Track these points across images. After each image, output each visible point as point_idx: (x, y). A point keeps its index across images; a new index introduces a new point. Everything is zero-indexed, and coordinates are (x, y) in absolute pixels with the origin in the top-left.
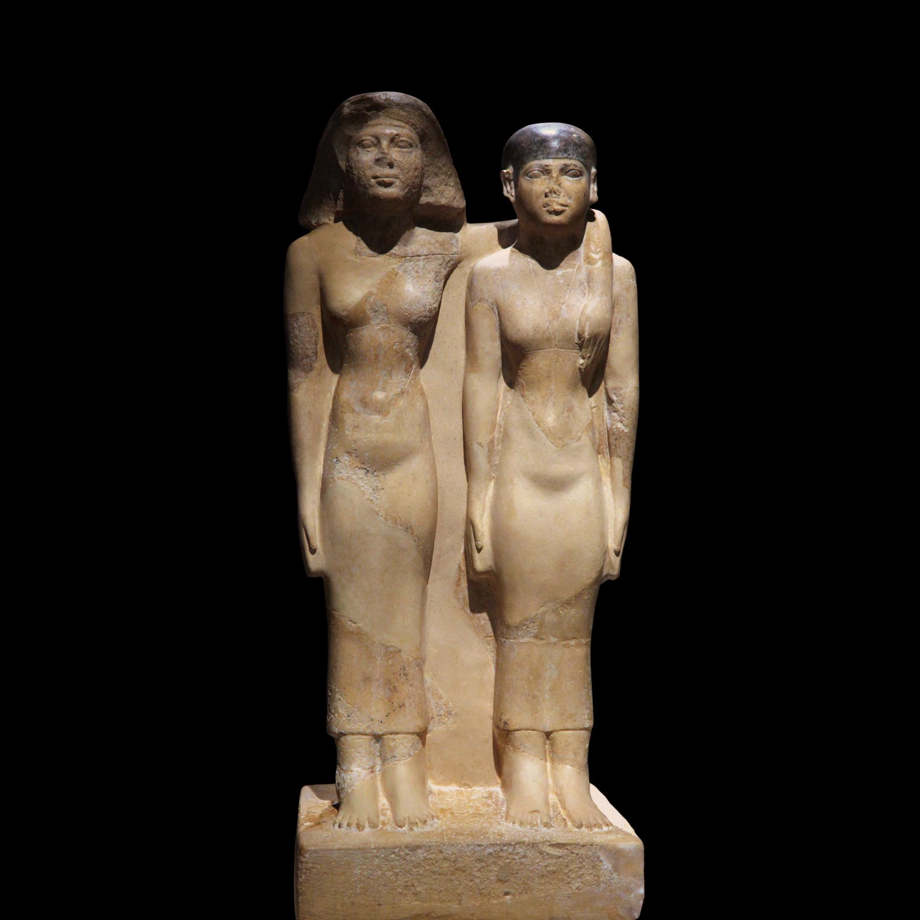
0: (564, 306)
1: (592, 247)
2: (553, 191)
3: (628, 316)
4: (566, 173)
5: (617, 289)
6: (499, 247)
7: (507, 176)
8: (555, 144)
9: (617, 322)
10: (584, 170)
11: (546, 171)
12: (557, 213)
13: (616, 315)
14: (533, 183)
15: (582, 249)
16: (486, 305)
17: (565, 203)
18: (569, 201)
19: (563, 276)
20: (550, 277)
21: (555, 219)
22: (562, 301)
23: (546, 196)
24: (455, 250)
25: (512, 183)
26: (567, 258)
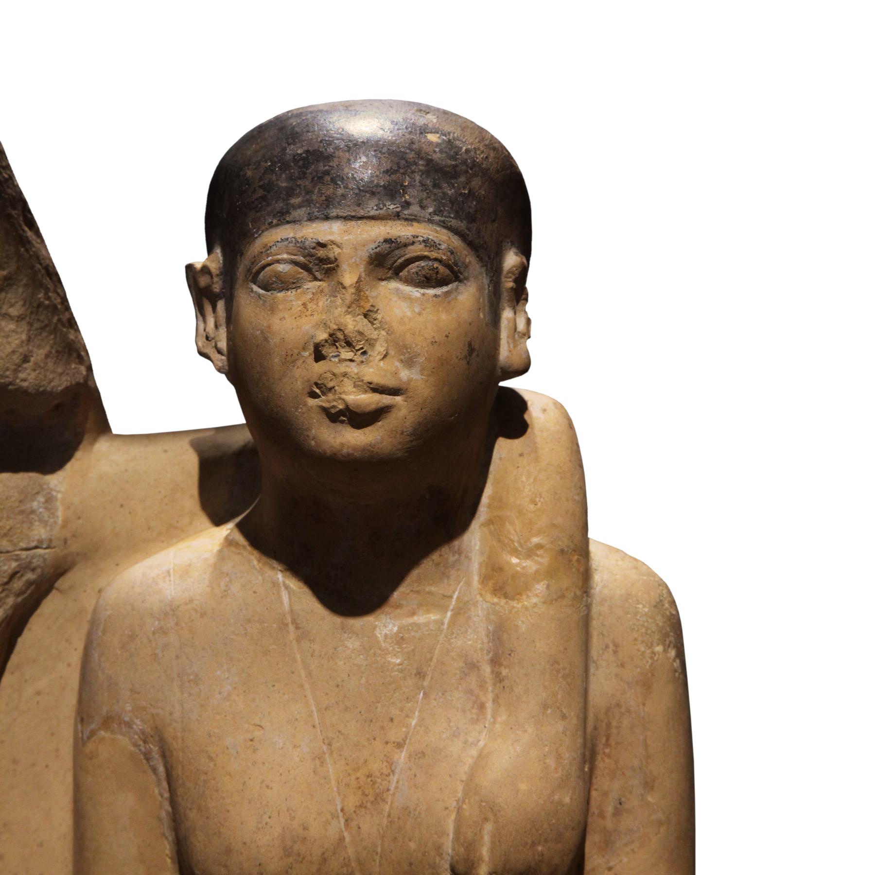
0: (402, 757)
1: (514, 530)
2: (339, 339)
3: (649, 785)
4: (396, 272)
5: (604, 684)
6: (203, 520)
7: (203, 281)
8: (363, 169)
9: (610, 810)
10: (470, 258)
11: (320, 264)
12: (359, 419)
13: (602, 782)
14: (273, 310)
15: (475, 538)
16: (124, 741)
17: (389, 382)
18: (405, 374)
19: (400, 639)
20: (353, 644)
21: (351, 439)
22: (394, 734)
23: (319, 356)
24: (40, 532)
25: (221, 305)
26: (415, 573)
